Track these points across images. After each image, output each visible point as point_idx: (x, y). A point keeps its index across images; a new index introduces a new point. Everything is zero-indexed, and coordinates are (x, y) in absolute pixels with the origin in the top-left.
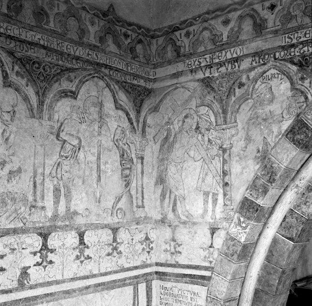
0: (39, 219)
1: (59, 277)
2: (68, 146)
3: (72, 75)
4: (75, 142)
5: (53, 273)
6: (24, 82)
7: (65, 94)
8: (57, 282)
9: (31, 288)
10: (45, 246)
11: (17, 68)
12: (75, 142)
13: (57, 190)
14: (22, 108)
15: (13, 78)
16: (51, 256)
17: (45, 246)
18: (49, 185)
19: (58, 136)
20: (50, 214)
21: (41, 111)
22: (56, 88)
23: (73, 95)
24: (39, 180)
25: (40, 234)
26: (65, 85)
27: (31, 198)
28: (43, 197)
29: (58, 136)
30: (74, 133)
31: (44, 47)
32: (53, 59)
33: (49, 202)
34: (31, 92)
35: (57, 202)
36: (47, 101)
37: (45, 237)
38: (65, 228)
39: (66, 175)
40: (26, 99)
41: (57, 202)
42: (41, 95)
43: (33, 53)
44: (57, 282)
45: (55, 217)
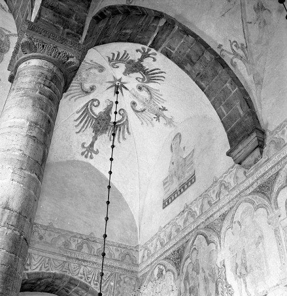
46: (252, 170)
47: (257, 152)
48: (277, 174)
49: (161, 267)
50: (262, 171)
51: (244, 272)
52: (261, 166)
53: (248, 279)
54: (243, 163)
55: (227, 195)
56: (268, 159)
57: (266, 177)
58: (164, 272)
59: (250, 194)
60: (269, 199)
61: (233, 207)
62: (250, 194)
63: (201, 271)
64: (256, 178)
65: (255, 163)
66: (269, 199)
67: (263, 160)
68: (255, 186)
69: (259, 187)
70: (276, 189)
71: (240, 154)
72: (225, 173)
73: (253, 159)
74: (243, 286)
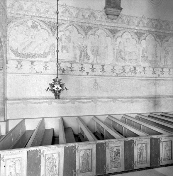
0: (161, 65)
1: (165, 77)
2: (167, 52)
3: (167, 37)
4: (168, 51)
5: (164, 76)
6: (158, 40)
7: (166, 41)
8: (165, 78)
9: (160, 78)
10: (162, 71)
11: (157, 37)
12: (168, 51)
13: (165, 60)
14: (158, 45)
15: (157, 39)
16: (163, 73)
17: (162, 71)
18: (163, 59)
19: (165, 50)
20: (163, 65)
21: (161, 45)
22: (164, 40)
23: (167, 41)
24: (161, 58)
25: (162, 68)
26: (166, 39)
27: (160, 62)
28: (162, 61)
29: (165, 50)
30: (168, 49)
31: (162, 32)
32: (163, 34)
33: (163, 63)
34: (160, 42)
35: (165, 63)
36: (163, 43)
37: (162, 69)
38: (166, 68)
39: (166, 58)
40: (159, 43)
41: (165, 63)
42: (161, 42)
43: (161, 34)
44: (165, 78)
45: (164, 65)
46: (110, 21)
47: (116, 17)
48: (119, 31)
49: (36, 23)
50: (114, 25)
51: (97, 54)
52: (114, 23)
53: (98, 57)
54: (108, 16)
55: (95, 21)
56: (117, 23)
57: (115, 28)
58: (39, 27)
59: (106, 29)
60: (114, 37)
61: (96, 28)
62: (106, 29)
63: (71, 42)
64: (110, 25)
65: (112, 19)
66: (114, 37)
67: (115, 21)
68: (109, 28)
69: (111, 29)
70: (117, 35)
71: (110, 11)
72: (96, 10)
73: (113, 18)
74: (95, 58)
